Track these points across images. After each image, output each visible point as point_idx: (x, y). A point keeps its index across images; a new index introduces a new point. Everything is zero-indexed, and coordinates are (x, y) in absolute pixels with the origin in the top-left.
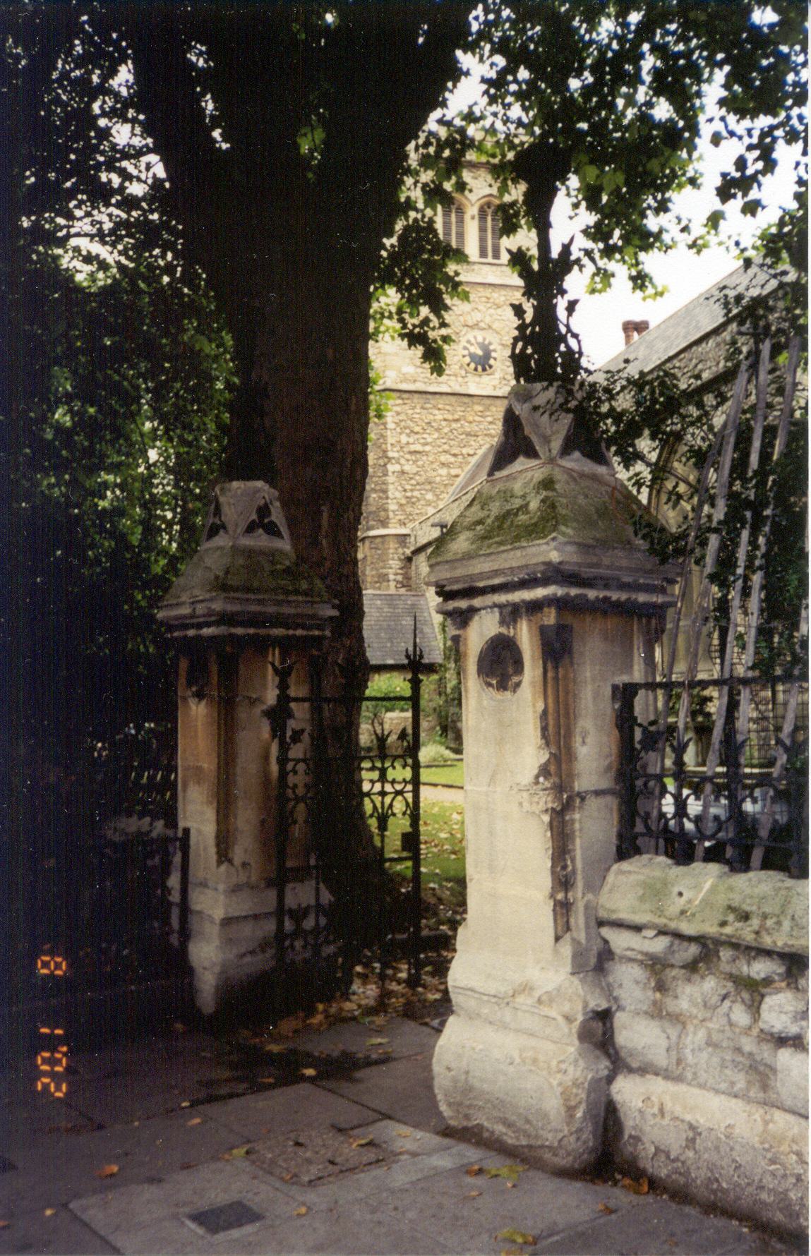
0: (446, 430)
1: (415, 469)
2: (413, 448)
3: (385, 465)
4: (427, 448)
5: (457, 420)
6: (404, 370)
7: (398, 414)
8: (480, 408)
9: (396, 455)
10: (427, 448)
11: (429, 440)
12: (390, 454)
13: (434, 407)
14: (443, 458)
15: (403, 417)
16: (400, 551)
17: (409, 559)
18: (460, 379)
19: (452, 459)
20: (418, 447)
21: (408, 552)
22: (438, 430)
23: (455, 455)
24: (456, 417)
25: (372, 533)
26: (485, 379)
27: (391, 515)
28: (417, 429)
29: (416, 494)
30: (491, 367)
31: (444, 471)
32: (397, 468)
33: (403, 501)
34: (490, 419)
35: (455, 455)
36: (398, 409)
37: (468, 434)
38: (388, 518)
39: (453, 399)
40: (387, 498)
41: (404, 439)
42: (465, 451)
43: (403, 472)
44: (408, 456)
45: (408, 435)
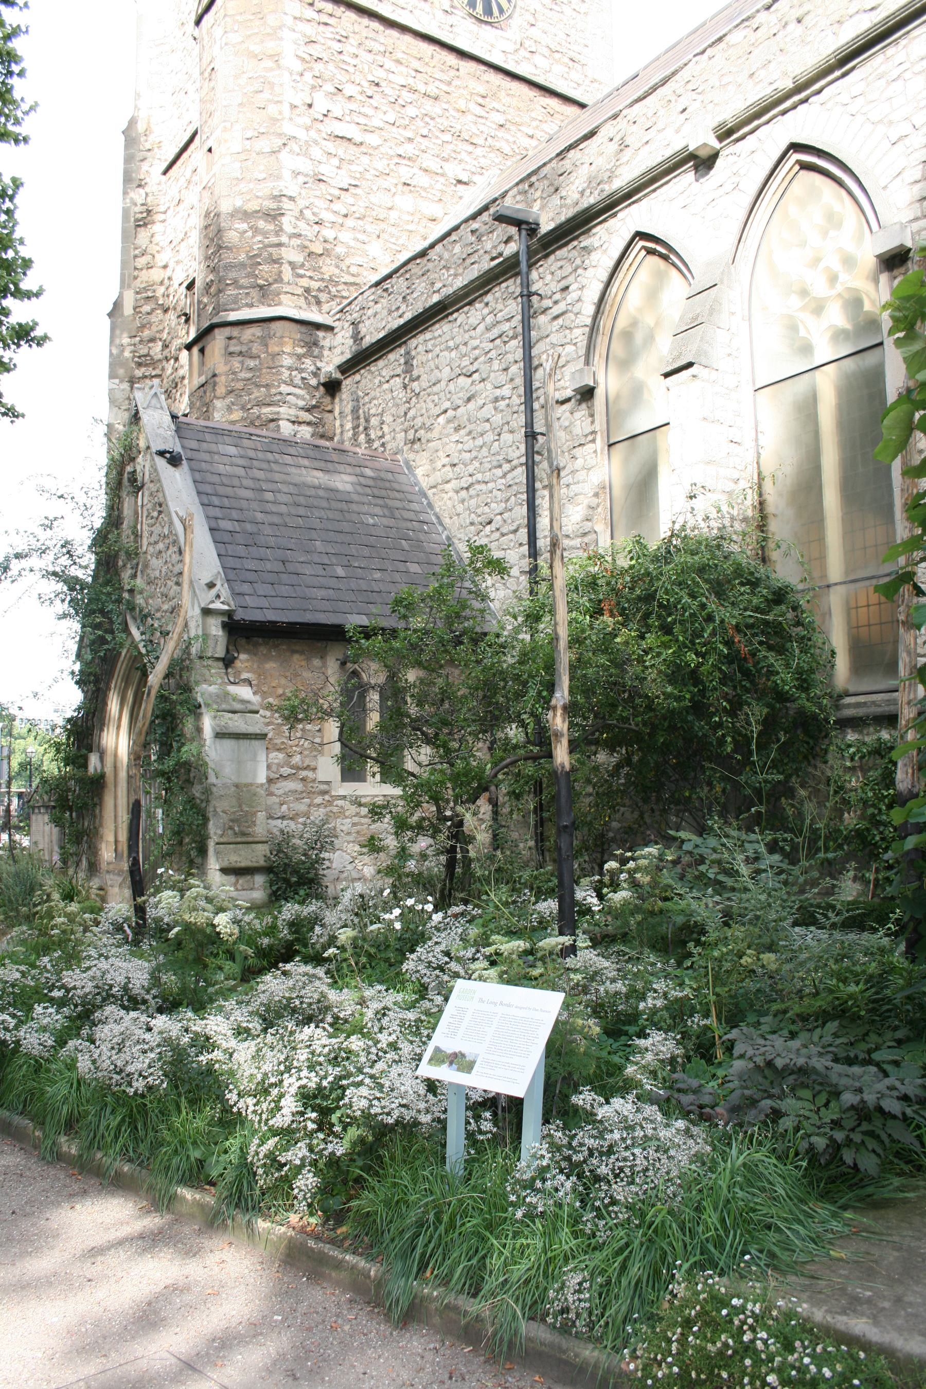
0: (411, 111)
8: (481, 89)
9: (301, 134)
10: (372, 139)
11: (376, 122)
14: (405, 172)
15: (316, 50)
16: (308, 364)
17: (332, 387)
21: (329, 366)
24: (432, 89)
25: (233, 316)
28: (349, 90)
31: (405, 202)
32: (303, 165)
38: (279, 280)
39: (428, 49)
40: (279, 231)
41: (322, 104)
44: (330, 146)
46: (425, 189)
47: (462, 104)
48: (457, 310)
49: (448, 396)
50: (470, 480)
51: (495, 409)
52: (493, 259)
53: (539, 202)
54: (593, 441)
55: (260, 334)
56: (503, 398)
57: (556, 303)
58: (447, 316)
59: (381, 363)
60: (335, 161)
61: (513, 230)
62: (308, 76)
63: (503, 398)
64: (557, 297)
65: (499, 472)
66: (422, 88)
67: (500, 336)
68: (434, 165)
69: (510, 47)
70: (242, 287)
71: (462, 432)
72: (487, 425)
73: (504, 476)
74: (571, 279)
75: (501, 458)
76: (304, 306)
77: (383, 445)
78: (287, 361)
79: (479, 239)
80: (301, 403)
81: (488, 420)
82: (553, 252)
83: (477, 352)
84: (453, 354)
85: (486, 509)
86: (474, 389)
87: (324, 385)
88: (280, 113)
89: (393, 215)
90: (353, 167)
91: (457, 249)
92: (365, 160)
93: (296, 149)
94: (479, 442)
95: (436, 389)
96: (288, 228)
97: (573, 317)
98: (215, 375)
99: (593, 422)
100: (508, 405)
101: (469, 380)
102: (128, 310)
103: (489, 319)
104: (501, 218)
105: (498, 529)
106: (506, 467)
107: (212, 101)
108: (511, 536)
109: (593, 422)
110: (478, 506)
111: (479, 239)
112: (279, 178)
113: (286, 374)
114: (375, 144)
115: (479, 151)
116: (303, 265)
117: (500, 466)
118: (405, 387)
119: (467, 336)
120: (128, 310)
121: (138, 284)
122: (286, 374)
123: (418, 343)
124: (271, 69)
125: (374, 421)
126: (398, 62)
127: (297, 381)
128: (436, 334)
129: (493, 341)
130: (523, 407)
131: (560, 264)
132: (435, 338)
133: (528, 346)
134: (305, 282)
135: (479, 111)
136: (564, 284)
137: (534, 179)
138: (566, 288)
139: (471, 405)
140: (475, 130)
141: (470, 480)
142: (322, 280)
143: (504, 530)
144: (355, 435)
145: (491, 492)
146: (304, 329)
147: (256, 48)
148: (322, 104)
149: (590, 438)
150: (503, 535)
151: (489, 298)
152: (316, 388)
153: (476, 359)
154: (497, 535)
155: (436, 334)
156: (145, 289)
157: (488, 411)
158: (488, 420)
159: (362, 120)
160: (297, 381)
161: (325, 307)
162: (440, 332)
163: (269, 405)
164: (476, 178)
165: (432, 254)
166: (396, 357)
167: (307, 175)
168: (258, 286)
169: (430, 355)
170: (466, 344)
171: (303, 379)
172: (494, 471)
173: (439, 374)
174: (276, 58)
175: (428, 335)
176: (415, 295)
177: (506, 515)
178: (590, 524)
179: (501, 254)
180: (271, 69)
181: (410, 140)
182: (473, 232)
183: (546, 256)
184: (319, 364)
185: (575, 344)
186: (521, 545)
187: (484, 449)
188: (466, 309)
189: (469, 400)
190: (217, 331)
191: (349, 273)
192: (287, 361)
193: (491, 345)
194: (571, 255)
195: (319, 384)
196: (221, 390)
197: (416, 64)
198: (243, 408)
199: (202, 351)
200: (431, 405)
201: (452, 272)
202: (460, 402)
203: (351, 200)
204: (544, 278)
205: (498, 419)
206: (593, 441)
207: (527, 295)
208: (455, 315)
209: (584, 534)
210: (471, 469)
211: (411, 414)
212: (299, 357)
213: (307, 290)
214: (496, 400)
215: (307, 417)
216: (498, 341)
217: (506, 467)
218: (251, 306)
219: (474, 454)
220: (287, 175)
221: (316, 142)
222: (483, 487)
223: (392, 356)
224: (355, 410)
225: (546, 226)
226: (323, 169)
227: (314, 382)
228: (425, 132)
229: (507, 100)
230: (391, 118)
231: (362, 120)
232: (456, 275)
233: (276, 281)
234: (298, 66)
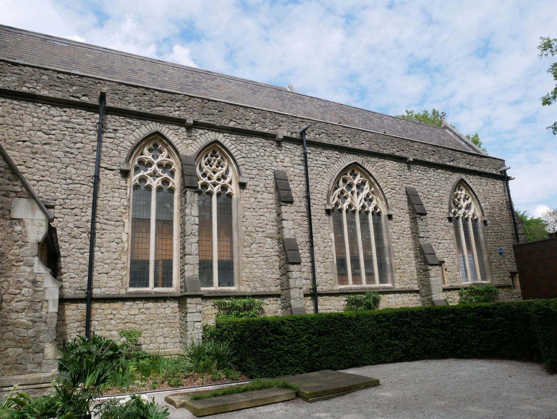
48: (43, 104)
49: (29, 136)
50: (41, 178)
52: (72, 96)
54: (126, 189)
56: (72, 153)
58: (34, 102)
63: (72, 153)
65: (64, 182)
67: (72, 128)
72: (59, 160)
81: (59, 158)
82: (111, 114)
83: (55, 127)
84: (36, 120)
85: (53, 194)
86: (50, 141)
94: (52, 165)
95: (17, 128)
101: (47, 136)
103: (65, 118)
105: (61, 205)
106: (69, 181)
108: (70, 210)
109: (126, 183)
117: (65, 180)
119: (48, 117)
128: (23, 105)
129: (67, 128)
131: (114, 120)
132: (21, 106)
138: (116, 130)
141: (41, 178)
145: (57, 188)
150: (64, 208)
153: (54, 130)
154: (60, 207)
155: (23, 105)
157: (60, 154)
158: (59, 158)
162: (26, 105)
169: (15, 111)
172: (62, 180)
173: (22, 123)
175: (15, 102)
177: (67, 201)
178: (120, 218)
188: (50, 106)
189: (45, 144)
193: (66, 129)
194: (120, 120)
205: (67, 160)
208: (40, 104)
210: (44, 174)
217: (69, 181)
219: (46, 168)
222: (51, 184)
225: (109, 104)
232: (43, 88)
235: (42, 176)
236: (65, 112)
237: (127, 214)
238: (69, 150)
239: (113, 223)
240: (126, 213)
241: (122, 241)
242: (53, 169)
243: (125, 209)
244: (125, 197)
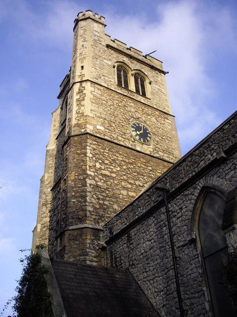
0: (125, 167)
1: (106, 187)
2: (104, 172)
3: (84, 179)
4: (114, 175)
5: (131, 164)
6: (98, 127)
7: (94, 149)
11: (114, 170)
12: (88, 172)
13: (117, 152)
15: (97, 152)
18: (131, 142)
19: (130, 186)
20: (107, 173)
22: (120, 165)
23: (130, 183)
25: (71, 228)
26: (145, 147)
27: (88, 214)
28: (106, 162)
29: (106, 203)
30: (148, 141)
31: (125, 192)
32: (93, 182)
33: (98, 206)
34: (150, 168)
35: (130, 183)
36: (95, 147)
37: (139, 173)
38: (86, 216)
42: (137, 183)
43: (97, 186)
44: (101, 177)
45: (100, 163)
46: (130, 188)
47: (139, 165)
48: (144, 220)
51: (161, 251)
52: (155, 203)
53: (168, 183)
55: (79, 233)
56: (163, 247)
57: (178, 213)
59: (120, 240)
60: (102, 181)
61: (161, 193)
62: (94, 158)
63: (163, 247)
64: (179, 211)
65: (164, 272)
66: (127, 161)
68: (132, 182)
69: (151, 150)
70: (74, 219)
71: (149, 260)
73: (166, 274)
74: (183, 205)
75: (164, 267)
76: (94, 224)
77: (122, 267)
78: (88, 241)
79: (150, 197)
80: (93, 255)
82: (175, 198)
84: (144, 234)
87: (101, 249)
88: (86, 168)
89: (121, 196)
90: (108, 183)
91: (143, 201)
92: (112, 181)
93: (91, 178)
94: (156, 263)
96: (88, 200)
97: (185, 217)
98: (65, 246)
99: (197, 251)
100: (165, 249)
102: (39, 230)
104: (158, 189)
106: (166, 270)
107: (66, 167)
109: (197, 251)
110: (157, 286)
111: (150, 197)
112: (86, 186)
113: (88, 245)
114: (114, 176)
115: (145, 178)
116: (93, 211)
118: (128, 247)
120: (39, 230)
121: (42, 222)
122: (88, 245)
123: (133, 232)
124: (83, 157)
125: (118, 259)
126: (120, 154)
127: (92, 248)
130: (170, 249)
133: (170, 228)
134: (94, 217)
135: (144, 166)
136: (180, 206)
137: (166, 177)
139: (151, 251)
140: (143, 172)
142: (99, 216)
143: (168, 293)
144: (112, 264)
146: (94, 231)
147: (79, 152)
148: (98, 165)
149: (196, 256)
151: (155, 215)
152: (98, 250)
156: (44, 224)
159: (110, 170)
160: (92, 248)
161: (101, 224)
163: (83, 256)
164: (145, 185)
165: (135, 204)
166: (125, 237)
167: (94, 185)
168: (79, 218)
170: (148, 231)
171: (94, 247)
174: (85, 154)
175: (135, 229)
176: (130, 217)
179: (157, 201)
180: (83, 157)
181: (124, 175)
182: (147, 196)
183: (173, 200)
184: (99, 242)
185: (187, 226)
186: (175, 298)
187: (158, 265)
189: (151, 249)
190: (66, 232)
191: (108, 214)
192: (88, 241)
195: (99, 248)
196: (67, 251)
197: (125, 155)
198: (74, 257)
199: (61, 239)
200: (137, 252)
201: (142, 208)
202: (148, 250)
203: (107, 192)
204: (173, 206)
206: (198, 257)
207: (168, 211)
209: (199, 292)
211: (131, 255)
212: (92, 240)
213: (95, 219)
214: (161, 248)
215: (95, 259)
216: (159, 228)
217: (166, 270)
218: (77, 224)
219: (154, 267)
220: (88, 185)
221: (96, 175)
222: (159, 278)
223: (123, 238)
224: (111, 256)
226: (99, 183)
227: (97, 248)
228: (129, 172)
229: (152, 163)
230: (119, 169)
231: (110, 170)
232: (143, 209)
233: (85, 216)
234: (91, 156)
235: (154, 275)
236: (154, 217)
237: (204, 282)
238: (161, 245)
239: (197, 295)
240: (203, 280)
241: (206, 311)
242: (158, 266)
243: (201, 277)
244: (199, 265)
